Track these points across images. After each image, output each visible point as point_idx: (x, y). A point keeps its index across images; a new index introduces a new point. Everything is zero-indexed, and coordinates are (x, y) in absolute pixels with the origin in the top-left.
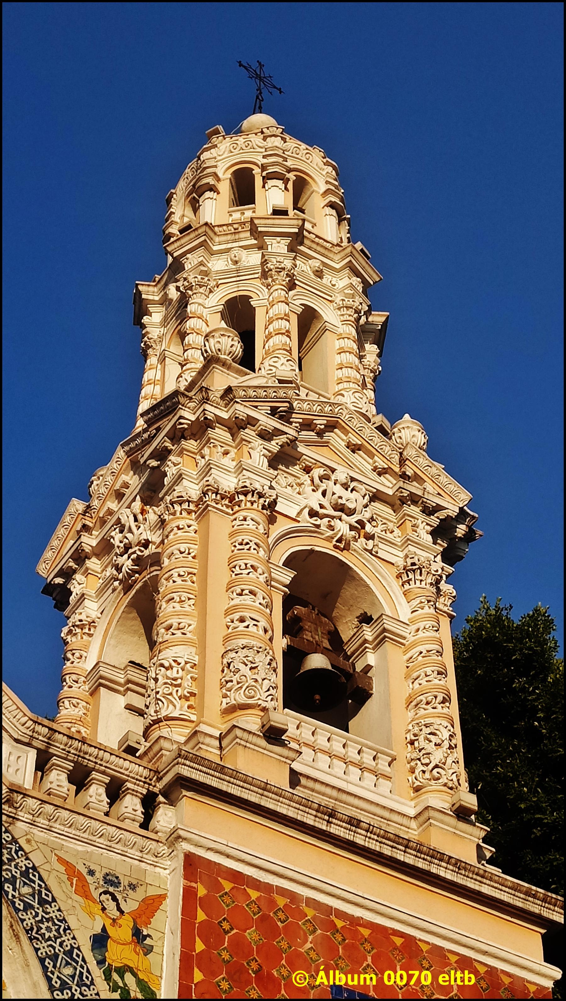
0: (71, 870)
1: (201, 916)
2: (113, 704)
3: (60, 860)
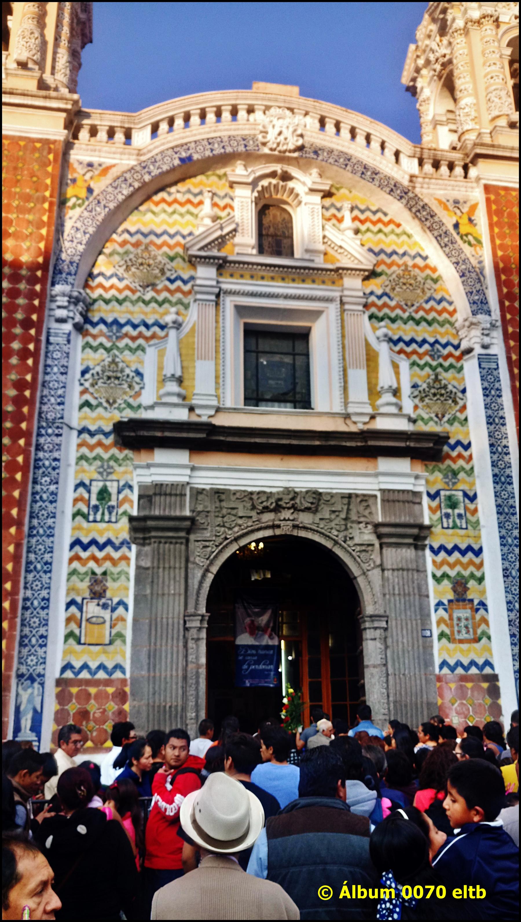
0: (440, 202)
1: (494, 207)
2: (443, 132)
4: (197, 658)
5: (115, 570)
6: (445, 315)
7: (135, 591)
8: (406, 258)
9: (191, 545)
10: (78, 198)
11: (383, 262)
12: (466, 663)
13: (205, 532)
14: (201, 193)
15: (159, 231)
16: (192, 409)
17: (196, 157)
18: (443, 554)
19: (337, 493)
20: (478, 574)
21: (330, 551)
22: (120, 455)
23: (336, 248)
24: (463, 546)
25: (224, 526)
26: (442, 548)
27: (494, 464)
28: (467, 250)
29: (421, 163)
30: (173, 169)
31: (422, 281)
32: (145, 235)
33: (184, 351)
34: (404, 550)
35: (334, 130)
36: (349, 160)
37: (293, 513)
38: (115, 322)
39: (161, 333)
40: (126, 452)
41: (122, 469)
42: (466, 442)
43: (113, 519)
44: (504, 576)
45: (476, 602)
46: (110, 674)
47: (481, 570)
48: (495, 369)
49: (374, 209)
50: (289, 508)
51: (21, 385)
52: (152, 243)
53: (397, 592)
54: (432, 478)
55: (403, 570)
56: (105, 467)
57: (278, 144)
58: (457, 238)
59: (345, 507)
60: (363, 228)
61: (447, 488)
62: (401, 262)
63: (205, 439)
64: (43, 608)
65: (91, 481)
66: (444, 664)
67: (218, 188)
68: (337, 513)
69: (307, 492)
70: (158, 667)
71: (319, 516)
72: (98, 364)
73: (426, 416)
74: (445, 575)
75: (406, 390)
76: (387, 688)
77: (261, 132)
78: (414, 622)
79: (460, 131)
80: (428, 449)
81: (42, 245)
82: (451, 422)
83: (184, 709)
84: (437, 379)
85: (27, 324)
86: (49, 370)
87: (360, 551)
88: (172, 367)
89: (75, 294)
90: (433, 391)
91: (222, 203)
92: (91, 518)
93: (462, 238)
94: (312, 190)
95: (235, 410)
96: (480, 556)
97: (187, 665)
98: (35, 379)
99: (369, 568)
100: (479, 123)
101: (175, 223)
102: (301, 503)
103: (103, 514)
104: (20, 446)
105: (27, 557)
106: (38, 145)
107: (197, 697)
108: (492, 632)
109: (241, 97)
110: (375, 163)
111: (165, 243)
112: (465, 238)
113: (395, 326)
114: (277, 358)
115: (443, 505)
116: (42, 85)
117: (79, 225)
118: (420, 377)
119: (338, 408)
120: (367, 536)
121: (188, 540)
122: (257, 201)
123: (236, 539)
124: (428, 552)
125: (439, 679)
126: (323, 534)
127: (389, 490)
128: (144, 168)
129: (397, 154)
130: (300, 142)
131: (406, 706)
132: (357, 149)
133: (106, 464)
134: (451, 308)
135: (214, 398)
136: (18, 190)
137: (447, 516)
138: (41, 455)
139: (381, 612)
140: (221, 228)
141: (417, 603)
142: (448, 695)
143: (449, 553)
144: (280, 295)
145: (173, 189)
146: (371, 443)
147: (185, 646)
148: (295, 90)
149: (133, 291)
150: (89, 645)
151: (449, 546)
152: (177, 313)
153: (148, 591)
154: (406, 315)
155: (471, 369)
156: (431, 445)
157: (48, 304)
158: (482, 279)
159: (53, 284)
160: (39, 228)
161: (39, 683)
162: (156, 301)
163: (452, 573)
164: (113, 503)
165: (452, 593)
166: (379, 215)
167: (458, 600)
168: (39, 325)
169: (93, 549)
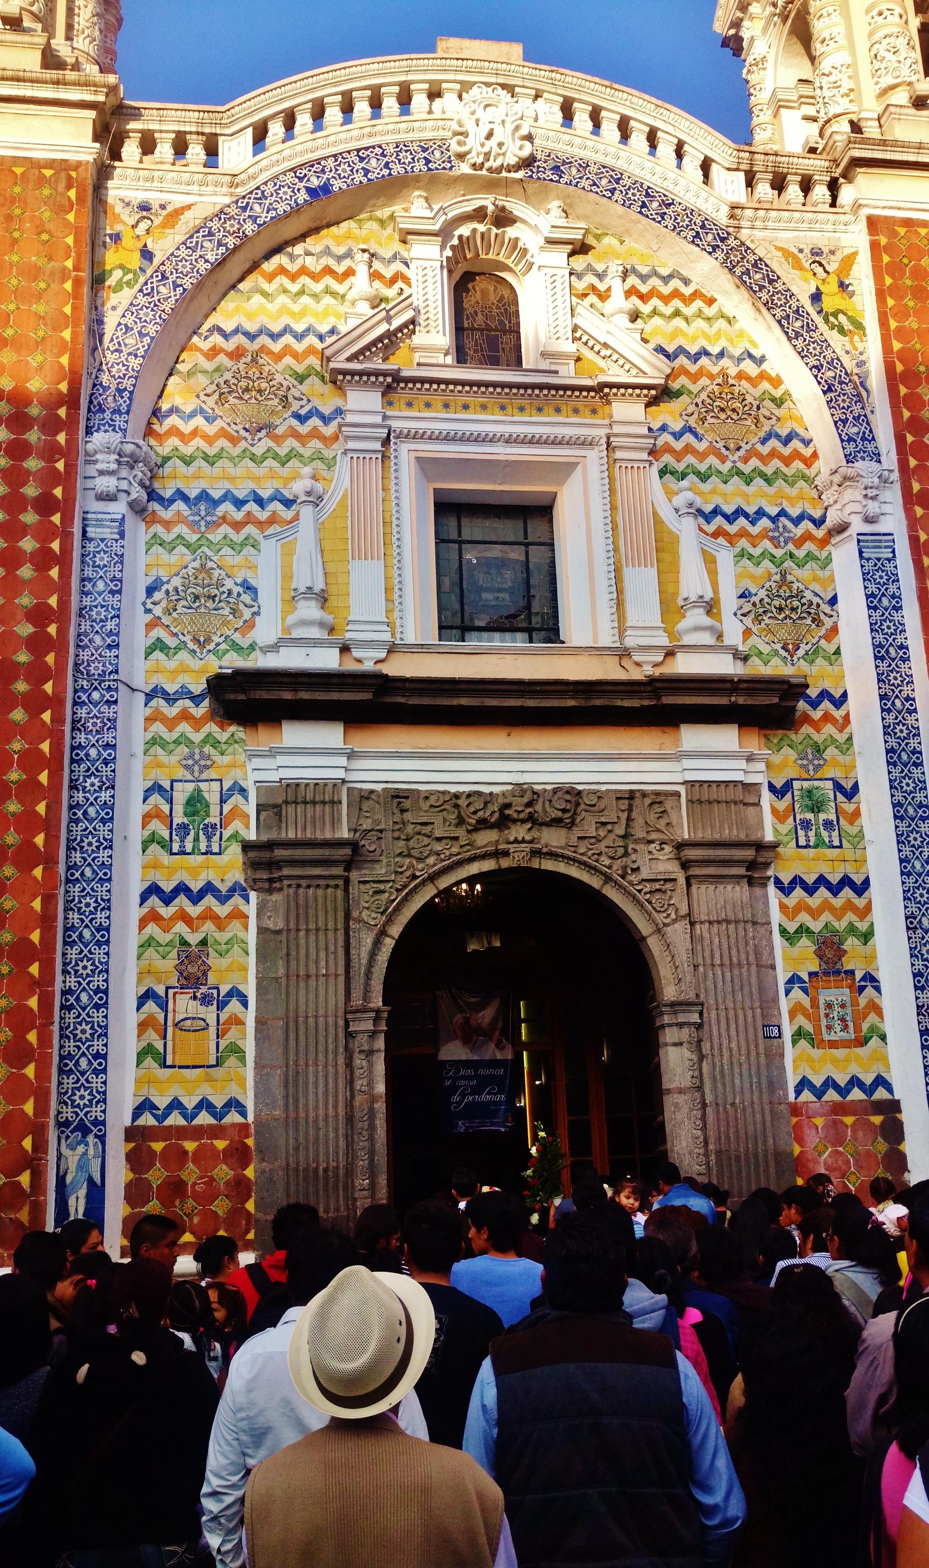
1: (886, 259)
3: (778, 248)
4: (371, 1084)
6: (798, 465)
7: (258, 972)
8: (725, 362)
9: (354, 890)
10: (126, 271)
11: (684, 371)
13: (377, 866)
14: (349, 254)
15: (276, 328)
16: (345, 649)
17: (337, 185)
18: (798, 892)
19: (608, 791)
20: (862, 926)
21: (598, 893)
22: (223, 736)
23: (596, 348)
24: (834, 879)
25: (409, 855)
26: (797, 881)
28: (836, 341)
29: (750, 183)
30: (297, 209)
31: (755, 404)
32: (252, 337)
33: (327, 546)
34: (729, 887)
35: (589, 125)
36: (618, 181)
37: (530, 829)
38: (204, 496)
39: (288, 514)
40: (233, 728)
41: (226, 759)
42: (837, 694)
43: (215, 849)
44: (908, 928)
45: (859, 975)
46: (219, 1116)
48: (889, 560)
49: (664, 272)
50: (523, 821)
52: (263, 348)
54: (776, 759)
55: (728, 922)
56: (197, 757)
58: (819, 320)
59: (624, 816)
60: (646, 309)
61: (805, 776)
62: (715, 370)
63: (370, 701)
64: (97, 1007)
65: (172, 781)
66: (803, 1084)
67: (381, 245)
68: (609, 827)
69: (555, 791)
70: (302, 1101)
71: (577, 832)
72: (177, 574)
73: (766, 649)
74: (803, 930)
75: (729, 602)
76: (704, 1128)
77: (456, 134)
79: (823, 118)
80: (767, 707)
81: (65, 360)
82: (810, 657)
83: (350, 1172)
85: (45, 505)
86: (89, 586)
87: (650, 892)
88: (308, 573)
89: (129, 448)
90: (776, 603)
91: (388, 273)
92: (176, 848)
93: (826, 320)
94: (550, 242)
95: (423, 648)
96: (866, 894)
97: (353, 1097)
98: (64, 602)
99: (667, 921)
100: (858, 100)
101: (303, 313)
102: (545, 811)
103: (196, 839)
105: (66, 918)
106: (48, 173)
107: (372, 1153)
109: (417, 69)
110: (665, 184)
112: (832, 319)
113: (706, 487)
114: (495, 552)
115: (797, 806)
116: (50, 60)
117: (129, 320)
118: (752, 577)
119: (607, 639)
120: (664, 864)
121: (347, 881)
122: (451, 266)
123: (432, 878)
124: (771, 889)
126: (585, 864)
127: (701, 783)
128: (244, 209)
129: (706, 166)
131: (738, 1158)
132: (633, 159)
133: (197, 751)
134: (807, 452)
135: (385, 628)
136: (15, 258)
137: (806, 825)
138: (81, 738)
139: (691, 996)
140: (388, 319)
141: (754, 981)
142: (813, 1139)
143: (810, 890)
144: (496, 439)
145: (298, 249)
146: (668, 700)
147: (349, 1064)
148: (516, 50)
149: (234, 441)
150: (180, 1067)
151: (810, 879)
152: (314, 478)
153: (281, 972)
154: (725, 468)
155: (844, 559)
156: (776, 700)
157: (81, 469)
158: (864, 394)
159: (89, 431)
160: (58, 328)
161: (96, 1136)
162: (276, 456)
163: (816, 926)
164: (214, 819)
165: (817, 961)
166: (675, 283)
167: (826, 973)
168: (67, 507)
169: (182, 901)
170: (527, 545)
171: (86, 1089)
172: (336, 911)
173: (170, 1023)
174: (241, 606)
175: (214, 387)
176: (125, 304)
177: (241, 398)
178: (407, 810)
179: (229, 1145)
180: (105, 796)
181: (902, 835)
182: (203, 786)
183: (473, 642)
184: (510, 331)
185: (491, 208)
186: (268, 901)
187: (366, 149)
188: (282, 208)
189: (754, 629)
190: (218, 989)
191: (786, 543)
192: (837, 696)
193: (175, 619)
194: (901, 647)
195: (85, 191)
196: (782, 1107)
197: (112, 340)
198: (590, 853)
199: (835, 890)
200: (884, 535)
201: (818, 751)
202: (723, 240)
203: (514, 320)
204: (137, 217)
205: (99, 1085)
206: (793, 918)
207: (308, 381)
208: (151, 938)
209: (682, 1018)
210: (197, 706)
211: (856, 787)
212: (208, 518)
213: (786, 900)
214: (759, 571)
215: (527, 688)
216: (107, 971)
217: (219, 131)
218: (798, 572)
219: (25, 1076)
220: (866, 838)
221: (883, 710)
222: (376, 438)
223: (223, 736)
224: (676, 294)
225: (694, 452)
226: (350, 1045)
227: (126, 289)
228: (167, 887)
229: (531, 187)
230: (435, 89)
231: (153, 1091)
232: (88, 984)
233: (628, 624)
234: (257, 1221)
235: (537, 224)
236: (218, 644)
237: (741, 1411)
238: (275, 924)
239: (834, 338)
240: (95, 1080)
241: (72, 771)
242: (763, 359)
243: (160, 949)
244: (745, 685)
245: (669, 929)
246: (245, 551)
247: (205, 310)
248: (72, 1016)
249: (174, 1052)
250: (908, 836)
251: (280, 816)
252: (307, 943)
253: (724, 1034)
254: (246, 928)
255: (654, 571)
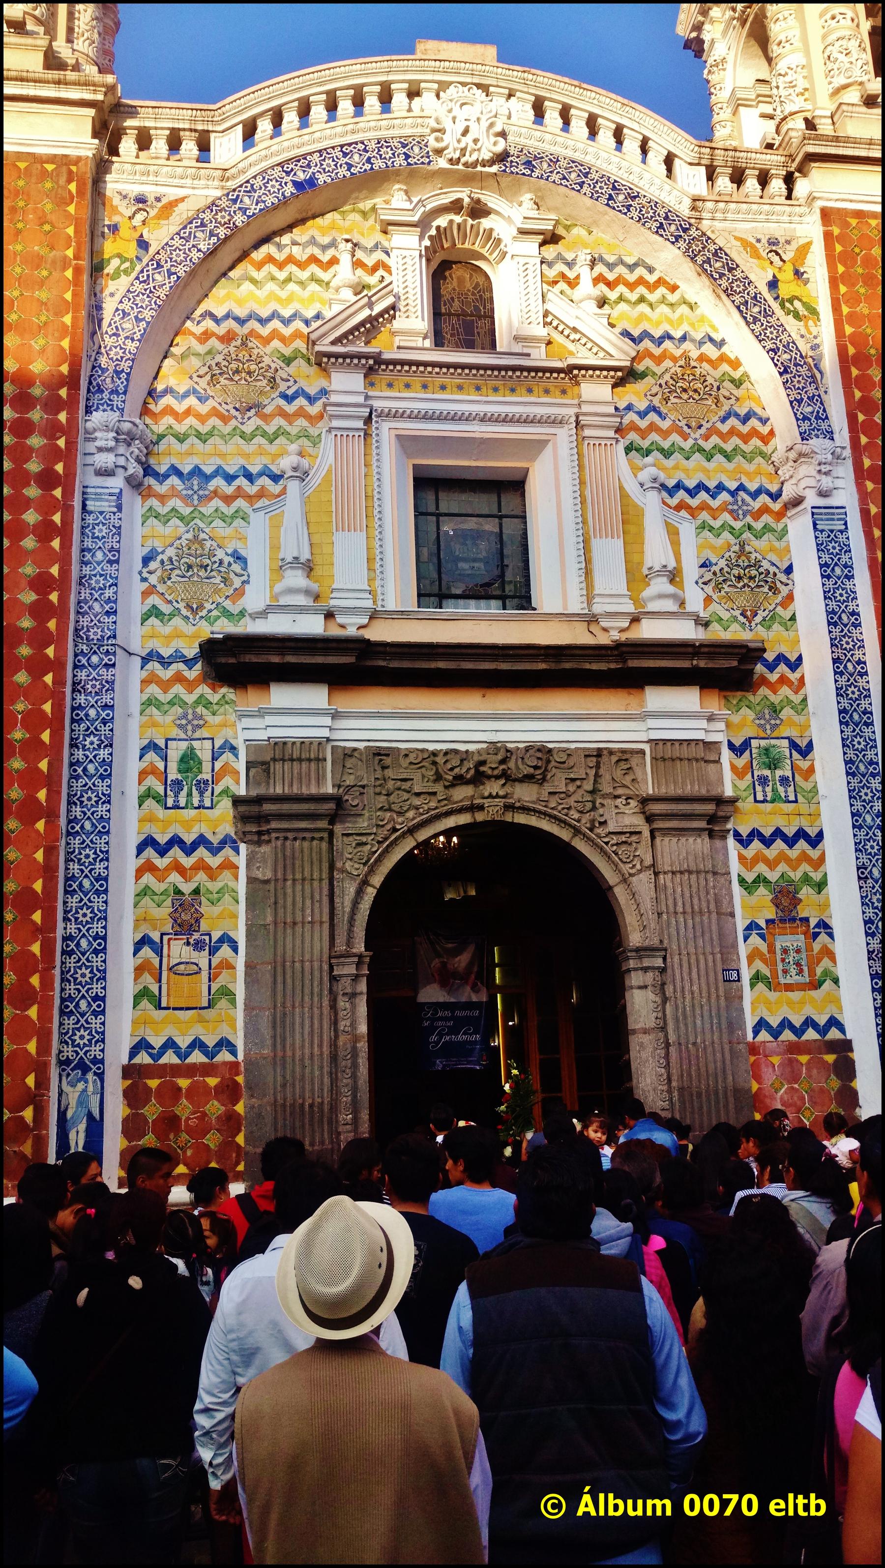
0: (745, 243)
1: (839, 248)
2: (750, 117)
3: (736, 238)
4: (353, 1025)
5: (214, 886)
6: (755, 442)
8: (687, 345)
9: (338, 843)
10: (123, 259)
11: (649, 354)
12: (797, 1022)
14: (333, 244)
15: (265, 313)
16: (329, 616)
17: (322, 178)
18: (756, 844)
20: (816, 876)
21: (567, 845)
22: (215, 698)
23: (566, 332)
24: (790, 831)
25: (390, 810)
26: (755, 834)
27: (840, 693)
28: (792, 325)
29: (711, 177)
30: (285, 202)
31: (715, 384)
32: (241, 322)
33: (313, 518)
34: (691, 840)
35: (560, 122)
36: (586, 175)
37: (504, 785)
38: (197, 471)
39: (275, 489)
40: (224, 690)
41: (217, 719)
42: (793, 658)
43: (207, 803)
44: (859, 878)
45: (813, 922)
46: (211, 1055)
47: (821, 869)
48: (841, 532)
49: (630, 261)
50: (497, 777)
51: (42, 583)
52: (252, 333)
53: (680, 909)
54: (736, 719)
55: (690, 872)
56: (190, 717)
57: (463, 151)
58: (775, 306)
59: (593, 771)
60: (613, 295)
61: (762, 735)
62: (678, 353)
63: (353, 665)
64: (96, 952)
65: (167, 740)
66: (761, 1025)
67: (363, 235)
68: (578, 783)
69: (527, 749)
71: (548, 788)
72: (171, 545)
73: (725, 615)
74: (760, 880)
75: (691, 571)
76: (667, 1066)
77: (434, 131)
78: (710, 958)
79: (779, 115)
80: (728, 670)
81: (66, 344)
82: (767, 623)
83: (334, 1108)
84: (742, 551)
85: (47, 480)
86: (88, 556)
87: (617, 844)
88: (294, 545)
89: (126, 426)
90: (735, 572)
91: (370, 261)
92: (170, 804)
93: (783, 306)
94: (523, 232)
95: (403, 615)
96: (820, 846)
97: (337, 1036)
98: (65, 572)
99: (633, 871)
100: (812, 99)
101: (290, 299)
102: (517, 768)
103: (190, 794)
104: (45, 685)
105: (67, 869)
106: (50, 167)
107: (355, 1089)
108: (841, 970)
109: (397, 70)
110: (631, 178)
111: (275, 334)
112: (787, 305)
113: (669, 463)
114: (471, 524)
115: (755, 763)
116: (52, 61)
117: (126, 306)
118: (713, 548)
119: (576, 606)
120: (630, 818)
121: (331, 834)
122: (429, 254)
123: (411, 831)
124: (731, 841)
125: (753, 1049)
126: (555, 817)
127: (665, 741)
128: (235, 201)
129: (669, 160)
130: (500, 147)
131: (699, 1095)
132: (601, 156)
133: (190, 711)
134: (765, 430)
136: (19, 248)
137: (764, 781)
138: (81, 699)
139: (655, 942)
140: (370, 305)
141: (714, 927)
142: (769, 1077)
143: (767, 842)
144: (471, 418)
145: (286, 239)
146: (633, 663)
147: (333, 1006)
148: (491, 52)
149: (225, 419)
150: (175, 1009)
151: (767, 832)
152: (301, 454)
153: (269, 919)
154: (687, 445)
155: (799, 532)
156: (735, 663)
157: (81, 446)
158: (818, 376)
159: (88, 411)
160: (59, 314)
161: (95, 1074)
162: (264, 434)
163: (773, 876)
164: (206, 775)
165: (774, 909)
166: (640, 271)
167: (783, 921)
168: (67, 482)
169: (176, 852)
170: (501, 517)
171: (86, 1029)
172: (321, 862)
173: (164, 967)
174: (232, 575)
175: (206, 369)
176: (123, 291)
177: (232, 380)
178: (387, 767)
179: (221, 1082)
180: (103, 753)
181: (854, 790)
182: (196, 744)
183: (450, 609)
184: (485, 317)
185: (467, 200)
186: (257, 853)
187: (350, 145)
188: (270, 200)
189: (715, 597)
190: (210, 935)
191: (744, 515)
192: (793, 659)
193: (170, 588)
194: (853, 613)
195: (85, 184)
196: (741, 1046)
197: (110, 325)
198: (560, 807)
199: (791, 842)
200: (837, 508)
201: (775, 711)
202: (685, 230)
203: (488, 306)
204: (134, 209)
205: (98, 1025)
206: (751, 868)
207: (295, 363)
208: (147, 887)
209: (646, 963)
210: (190, 669)
211: (810, 745)
212: (201, 493)
213: (744, 852)
214: (719, 542)
215: (501, 652)
216: (105, 919)
217: (210, 128)
218: (756, 543)
219: (28, 1017)
220: (820, 793)
221: (836, 673)
222: (359, 417)
223: (215, 698)
224: (641, 281)
225: (658, 430)
226: (335, 988)
227: (123, 277)
228: (162, 839)
229: (505, 181)
230: (414, 88)
231: (149, 1031)
232: (88, 930)
233: (596, 592)
234: (247, 1153)
235: (510, 215)
236: (210, 611)
237: (702, 1332)
238: (264, 874)
239: (789, 322)
240: (94, 1021)
241: (72, 730)
242: (722, 343)
243: (156, 898)
244: (706, 650)
245: (634, 879)
246: (235, 524)
247: (198, 297)
248: (73, 960)
249: (168, 995)
250: (860, 791)
251: (269, 773)
252: (294, 892)
253: (686, 977)
254: (237, 878)
255: (620, 543)
